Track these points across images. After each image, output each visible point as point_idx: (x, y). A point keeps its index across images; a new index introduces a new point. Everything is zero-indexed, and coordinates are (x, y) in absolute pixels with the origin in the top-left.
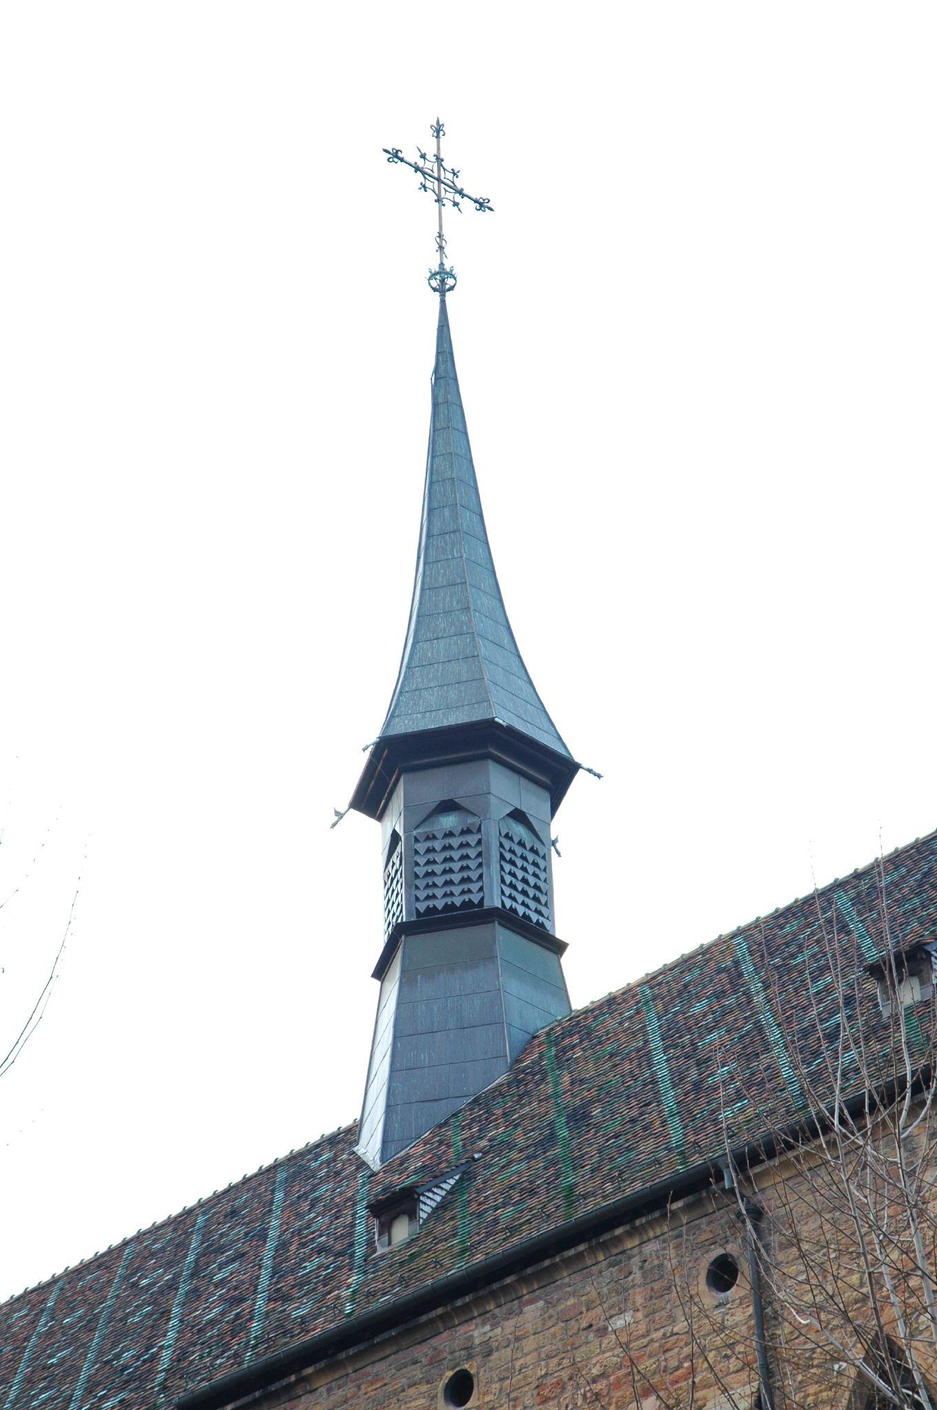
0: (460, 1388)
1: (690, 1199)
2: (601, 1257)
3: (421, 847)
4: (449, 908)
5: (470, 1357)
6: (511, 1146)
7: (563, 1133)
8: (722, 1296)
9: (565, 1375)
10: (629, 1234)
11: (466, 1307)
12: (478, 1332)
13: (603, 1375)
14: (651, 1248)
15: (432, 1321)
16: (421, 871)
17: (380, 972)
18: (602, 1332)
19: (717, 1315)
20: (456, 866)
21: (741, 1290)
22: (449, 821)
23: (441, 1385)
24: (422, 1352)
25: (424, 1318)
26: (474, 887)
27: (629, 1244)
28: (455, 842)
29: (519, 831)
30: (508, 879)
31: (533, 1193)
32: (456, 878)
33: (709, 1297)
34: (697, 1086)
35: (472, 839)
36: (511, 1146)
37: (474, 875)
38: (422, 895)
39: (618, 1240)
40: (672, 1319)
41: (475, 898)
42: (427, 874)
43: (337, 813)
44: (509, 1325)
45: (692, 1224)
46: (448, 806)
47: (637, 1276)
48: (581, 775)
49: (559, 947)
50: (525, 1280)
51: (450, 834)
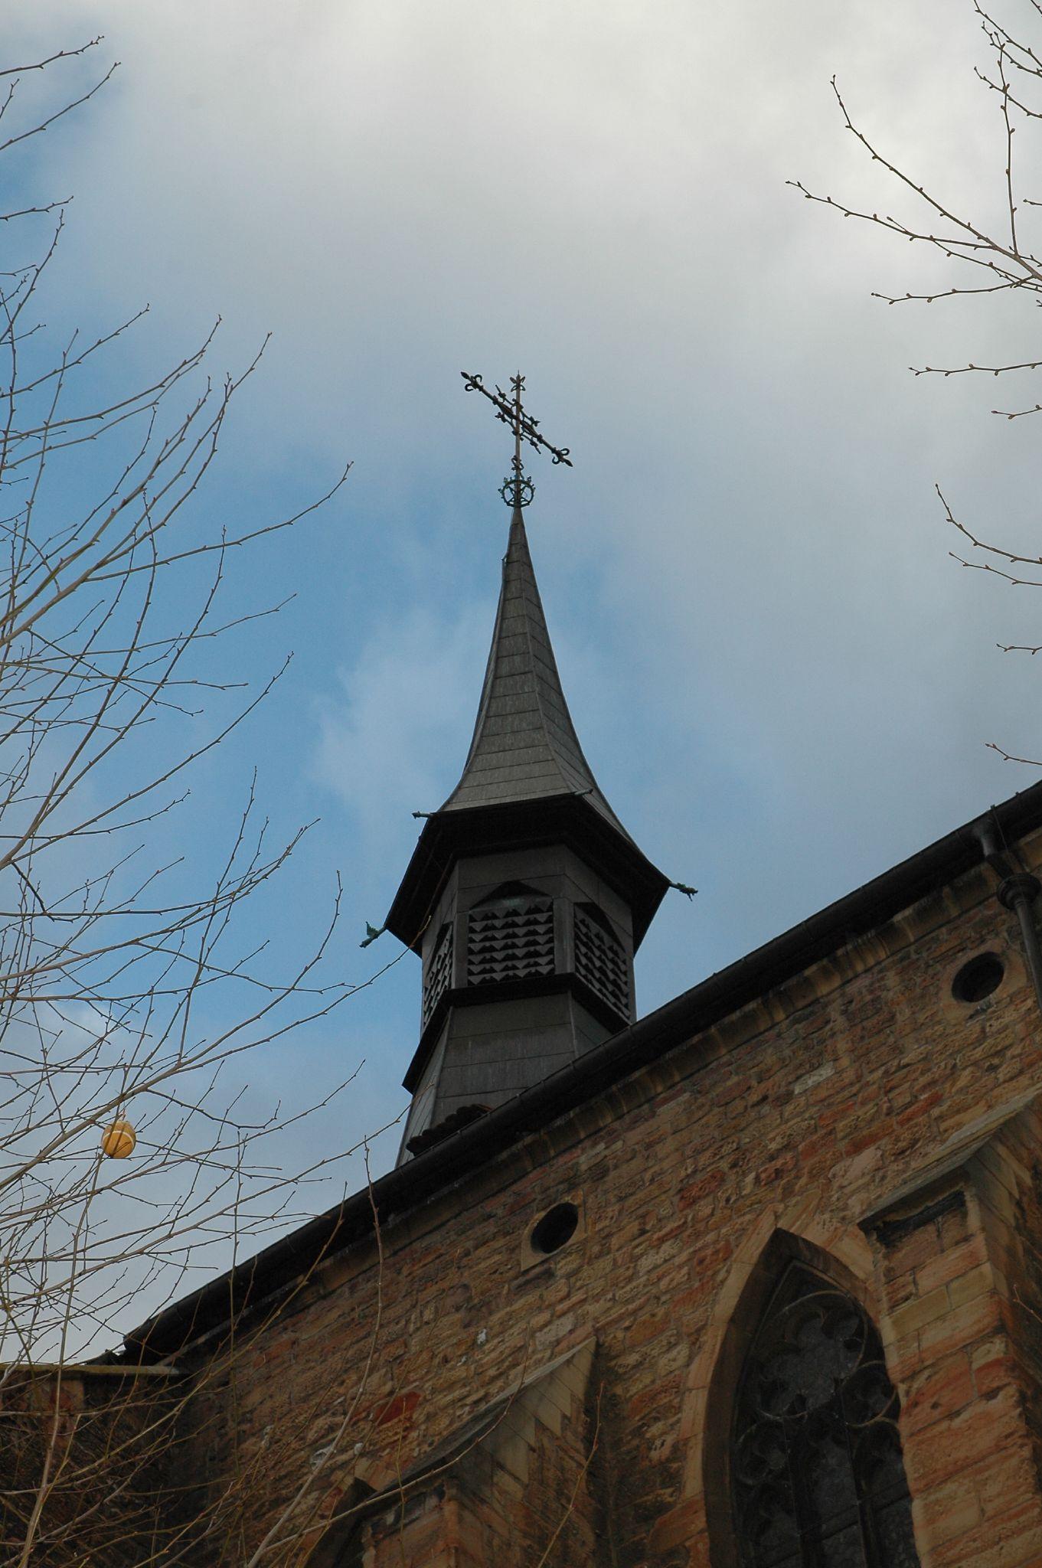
1: (924, 901)
2: (780, 1015)
10: (826, 974)
12: (584, 1159)
13: (786, 1147)
16: (476, 947)
18: (788, 1096)
19: (974, 1027)
23: (527, 1232)
24: (497, 1206)
27: (823, 989)
30: (584, 961)
33: (952, 1010)
39: (808, 983)
42: (483, 950)
43: (370, 931)
45: (922, 940)
46: (513, 889)
47: (839, 1021)
48: (671, 895)
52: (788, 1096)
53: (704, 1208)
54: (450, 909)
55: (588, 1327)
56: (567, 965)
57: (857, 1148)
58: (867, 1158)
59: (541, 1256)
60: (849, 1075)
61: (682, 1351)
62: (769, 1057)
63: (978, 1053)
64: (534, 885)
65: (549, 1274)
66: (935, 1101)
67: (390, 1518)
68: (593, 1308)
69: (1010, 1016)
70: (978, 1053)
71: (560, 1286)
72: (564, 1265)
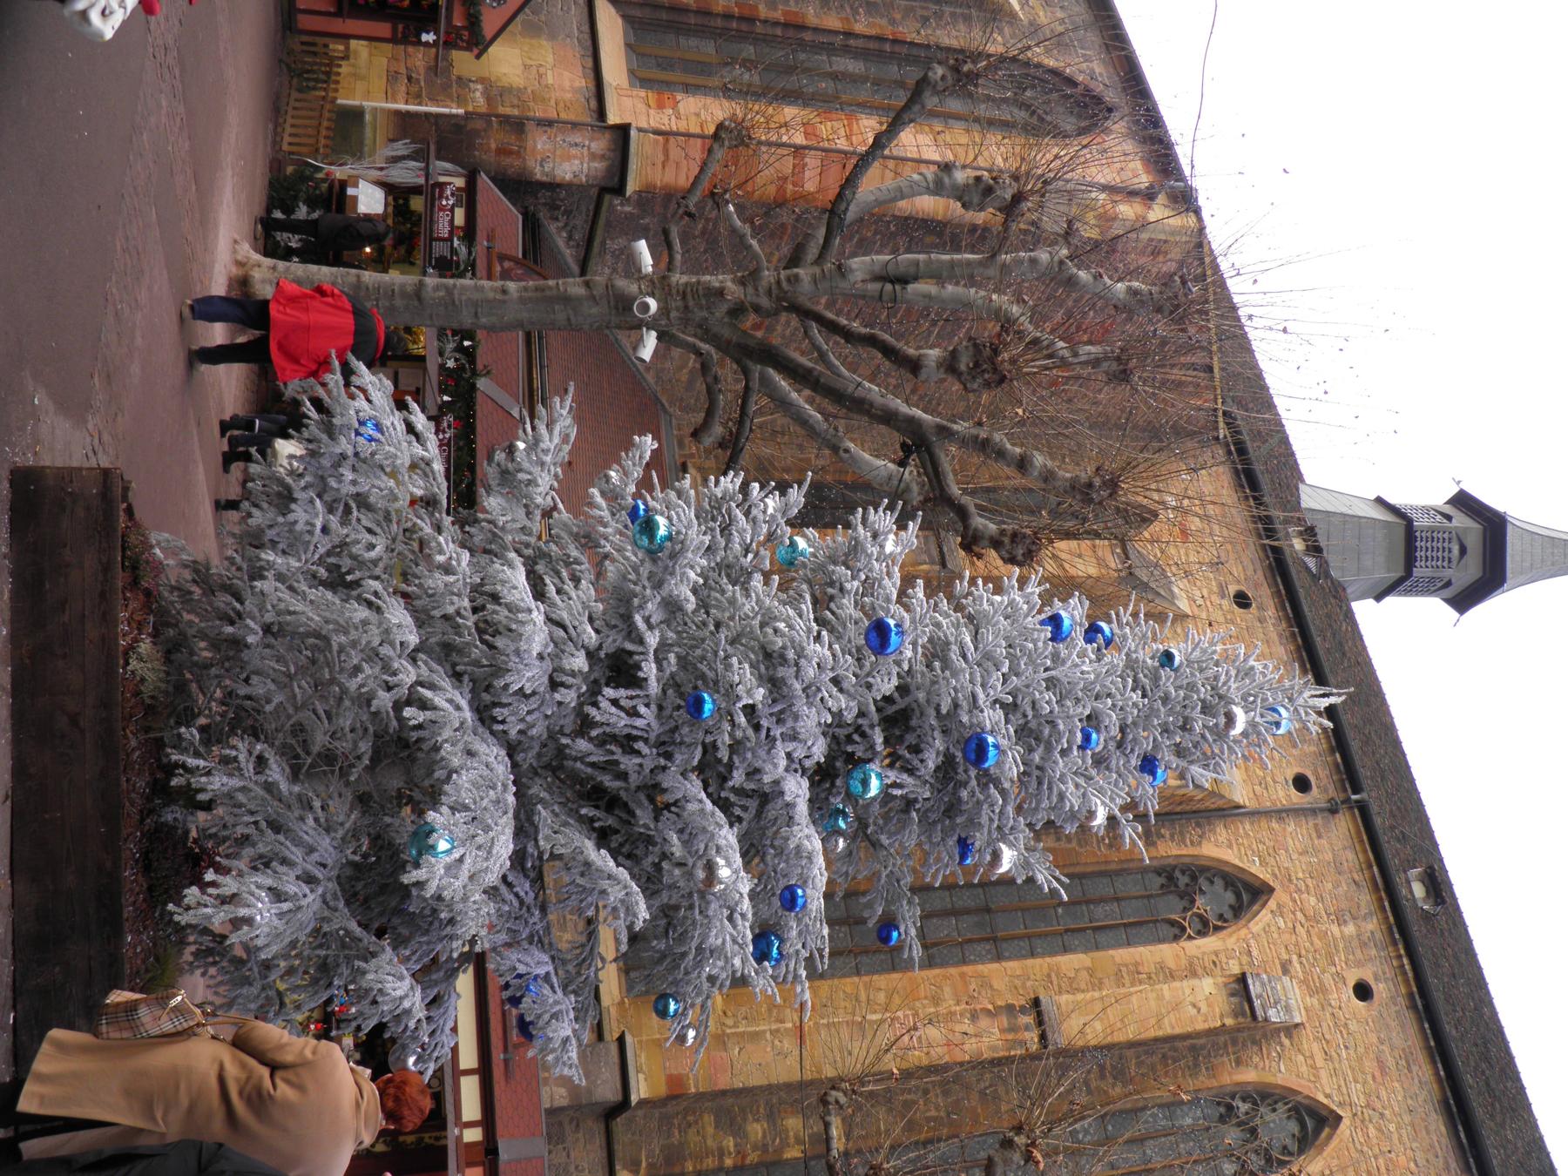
0: (1242, 600)
1: (1342, 768)
5: (1258, 608)
8: (1291, 782)
11: (1284, 609)
12: (1271, 612)
15: (1277, 585)
16: (1435, 535)
17: (1380, 501)
19: (1280, 779)
20: (1434, 554)
21: (1296, 797)
22: (1456, 549)
23: (1243, 588)
25: (1279, 580)
26: (1423, 563)
32: (1429, 553)
33: (1290, 774)
35: (1445, 564)
37: (1429, 563)
38: (1424, 535)
41: (1417, 564)
43: (1459, 482)
49: (1379, 598)
50: (1298, 649)
51: (1450, 551)
54: (1461, 521)
56: (1417, 572)
63: (1269, 779)
64: (1463, 561)
65: (1223, 597)
67: (1118, 550)
69: (1281, 794)
70: (1269, 779)
71: (1216, 599)
72: (1225, 603)
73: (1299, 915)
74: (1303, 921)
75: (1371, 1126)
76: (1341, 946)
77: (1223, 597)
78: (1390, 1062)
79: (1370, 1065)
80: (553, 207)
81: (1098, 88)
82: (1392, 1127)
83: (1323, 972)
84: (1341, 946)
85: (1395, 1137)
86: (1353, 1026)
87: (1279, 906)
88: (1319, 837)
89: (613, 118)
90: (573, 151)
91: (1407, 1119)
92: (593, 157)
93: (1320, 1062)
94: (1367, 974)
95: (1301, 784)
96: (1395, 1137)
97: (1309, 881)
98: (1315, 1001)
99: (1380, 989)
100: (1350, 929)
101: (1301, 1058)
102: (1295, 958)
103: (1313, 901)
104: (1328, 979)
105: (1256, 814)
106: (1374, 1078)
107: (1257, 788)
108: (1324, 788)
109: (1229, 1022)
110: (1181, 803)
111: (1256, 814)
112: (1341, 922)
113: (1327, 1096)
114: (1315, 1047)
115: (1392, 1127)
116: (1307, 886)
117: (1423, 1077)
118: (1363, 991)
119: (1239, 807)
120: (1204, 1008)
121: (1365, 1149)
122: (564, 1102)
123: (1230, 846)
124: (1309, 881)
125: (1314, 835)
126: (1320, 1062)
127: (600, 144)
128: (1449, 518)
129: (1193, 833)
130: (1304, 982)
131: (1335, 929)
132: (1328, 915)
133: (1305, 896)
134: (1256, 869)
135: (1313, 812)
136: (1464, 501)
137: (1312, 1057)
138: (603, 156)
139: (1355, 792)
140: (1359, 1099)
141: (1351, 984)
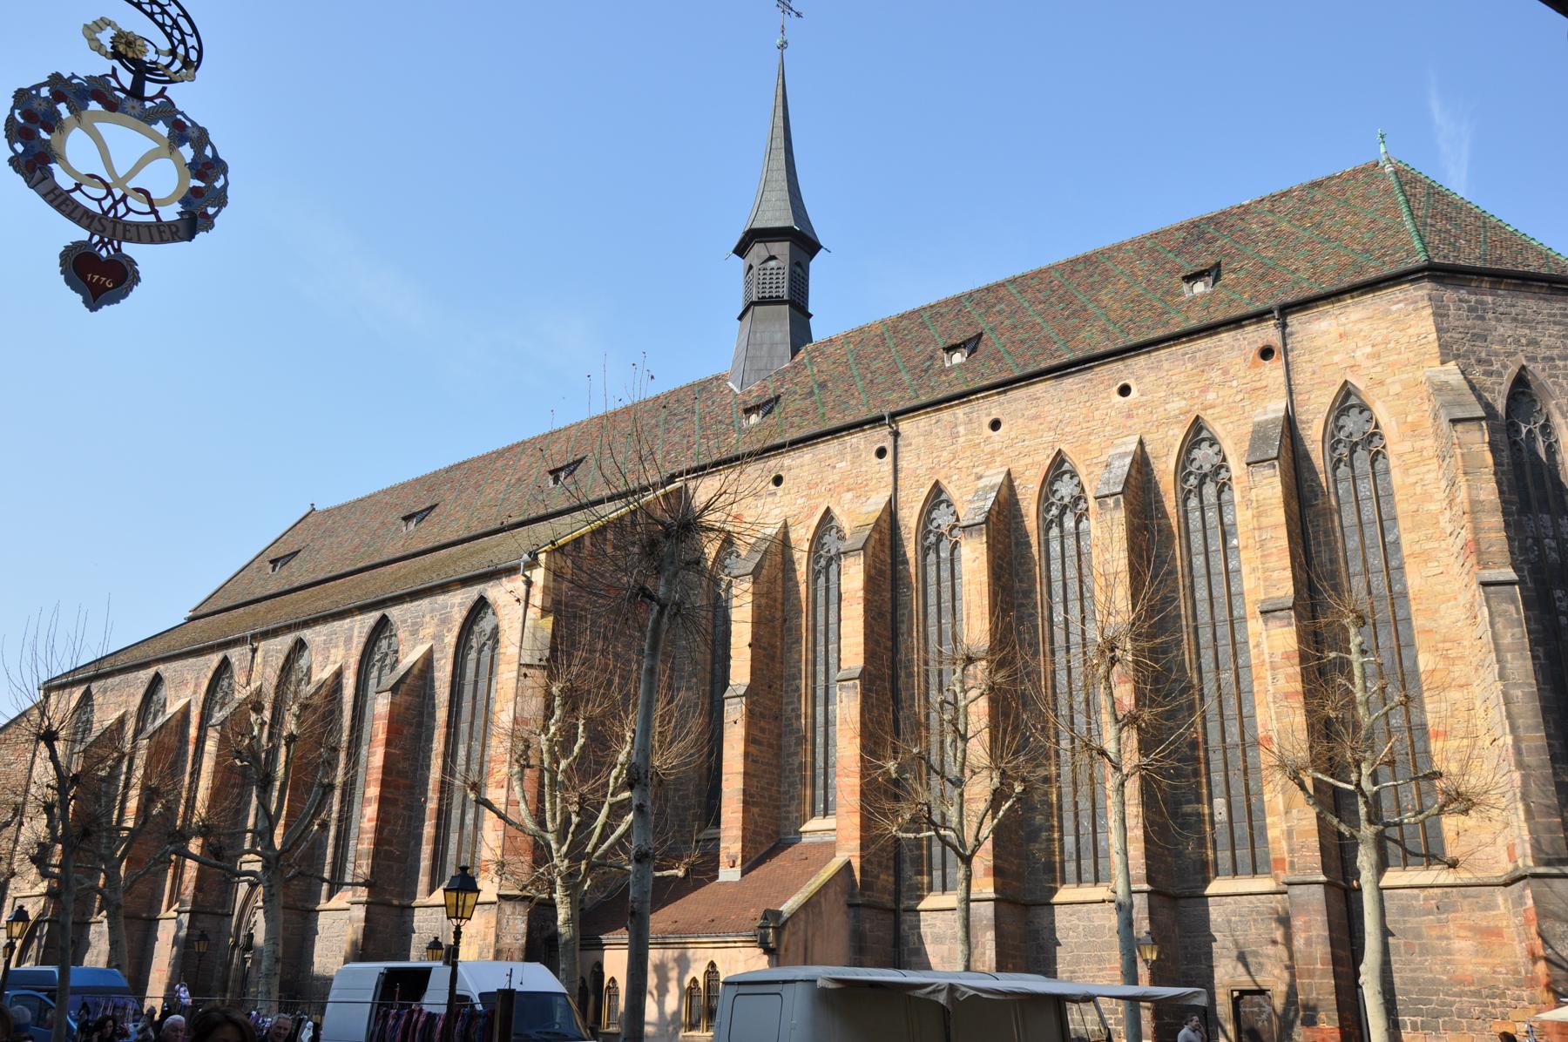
0: (778, 481)
3: (761, 273)
4: (771, 297)
6: (795, 393)
7: (816, 391)
8: (880, 460)
9: (819, 481)
10: (847, 435)
13: (833, 482)
14: (854, 440)
17: (740, 318)
19: (877, 467)
21: (889, 457)
22: (772, 264)
28: (775, 272)
29: (799, 270)
31: (807, 413)
34: (872, 381)
36: (795, 393)
38: (761, 291)
40: (861, 466)
44: (799, 461)
47: (849, 449)
49: (810, 316)
51: (772, 269)
52: (834, 467)
53: (813, 491)
55: (783, 514)
57: (849, 490)
58: (849, 495)
59: (772, 487)
60: (849, 468)
61: (804, 530)
62: (832, 452)
63: (878, 476)
66: (867, 485)
68: (786, 509)
70: (878, 476)
71: (777, 499)
73: (952, 464)
74: (955, 461)
75: (1066, 430)
76: (970, 437)
77: (775, 494)
78: (1033, 411)
79: (1034, 425)
80: (542, 928)
81: (470, 603)
82: (1068, 415)
83: (983, 451)
84: (970, 437)
85: (1073, 414)
86: (1013, 435)
87: (946, 478)
88: (910, 444)
89: (495, 899)
90: (511, 924)
91: (1063, 404)
92: (513, 913)
93: (1028, 460)
94: (987, 421)
95: (881, 453)
96: (1073, 414)
97: (934, 455)
98: (998, 459)
99: (995, 414)
100: (961, 429)
101: (1027, 473)
102: (975, 470)
103: (945, 454)
104: (988, 449)
105: (896, 489)
106: (1041, 424)
107: (882, 485)
108: (881, 436)
109: (984, 539)
110: (883, 545)
111: (896, 489)
112: (955, 436)
113: (1048, 456)
114: (1022, 462)
115: (1068, 415)
116: (937, 457)
117: (1040, 388)
118: (995, 425)
119: (890, 499)
120: (976, 554)
121: (1077, 435)
122: (993, 933)
123: (912, 507)
124: (934, 455)
125: (909, 448)
126: (1028, 460)
127: (508, 907)
128: (751, 267)
129: (904, 533)
130: (988, 465)
131: (961, 440)
132: (953, 444)
133: (942, 459)
134: (925, 491)
135: (896, 447)
136: (741, 250)
137: (1027, 465)
138: (514, 908)
139: (884, 419)
140: (1049, 437)
141: (991, 431)
